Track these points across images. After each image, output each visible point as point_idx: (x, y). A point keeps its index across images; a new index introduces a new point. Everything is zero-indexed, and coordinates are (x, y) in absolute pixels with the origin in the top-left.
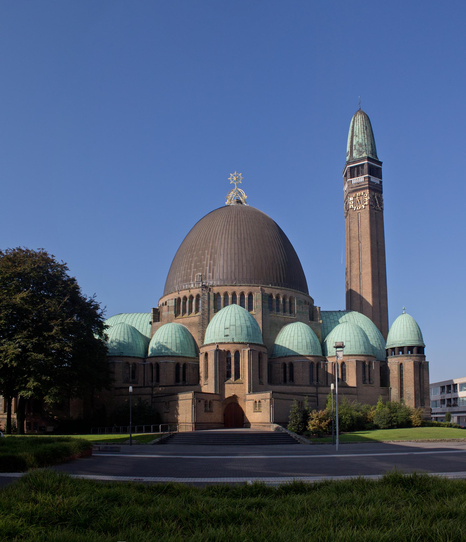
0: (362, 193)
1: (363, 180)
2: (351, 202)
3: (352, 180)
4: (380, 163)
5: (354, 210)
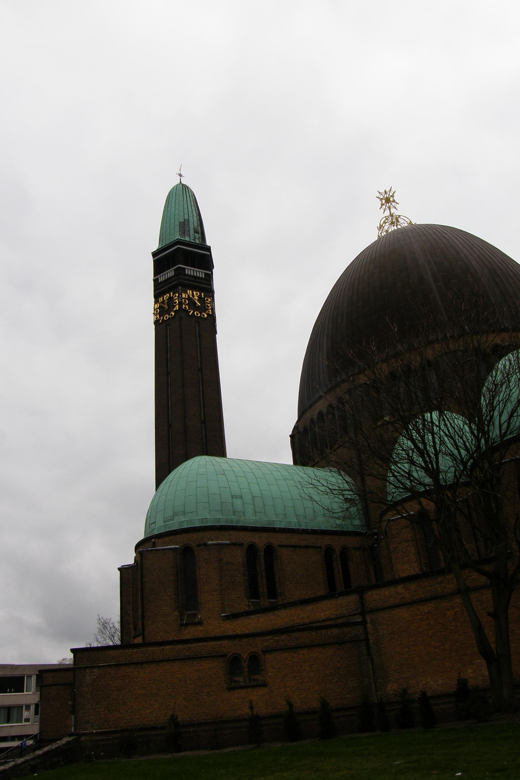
0: (203, 294)
1: (203, 276)
2: (185, 301)
3: (185, 269)
4: (213, 267)
5: (190, 314)
